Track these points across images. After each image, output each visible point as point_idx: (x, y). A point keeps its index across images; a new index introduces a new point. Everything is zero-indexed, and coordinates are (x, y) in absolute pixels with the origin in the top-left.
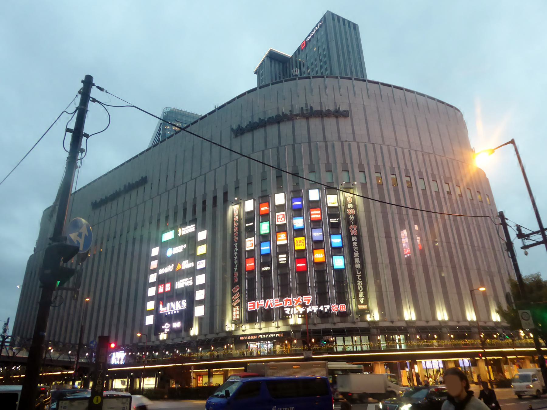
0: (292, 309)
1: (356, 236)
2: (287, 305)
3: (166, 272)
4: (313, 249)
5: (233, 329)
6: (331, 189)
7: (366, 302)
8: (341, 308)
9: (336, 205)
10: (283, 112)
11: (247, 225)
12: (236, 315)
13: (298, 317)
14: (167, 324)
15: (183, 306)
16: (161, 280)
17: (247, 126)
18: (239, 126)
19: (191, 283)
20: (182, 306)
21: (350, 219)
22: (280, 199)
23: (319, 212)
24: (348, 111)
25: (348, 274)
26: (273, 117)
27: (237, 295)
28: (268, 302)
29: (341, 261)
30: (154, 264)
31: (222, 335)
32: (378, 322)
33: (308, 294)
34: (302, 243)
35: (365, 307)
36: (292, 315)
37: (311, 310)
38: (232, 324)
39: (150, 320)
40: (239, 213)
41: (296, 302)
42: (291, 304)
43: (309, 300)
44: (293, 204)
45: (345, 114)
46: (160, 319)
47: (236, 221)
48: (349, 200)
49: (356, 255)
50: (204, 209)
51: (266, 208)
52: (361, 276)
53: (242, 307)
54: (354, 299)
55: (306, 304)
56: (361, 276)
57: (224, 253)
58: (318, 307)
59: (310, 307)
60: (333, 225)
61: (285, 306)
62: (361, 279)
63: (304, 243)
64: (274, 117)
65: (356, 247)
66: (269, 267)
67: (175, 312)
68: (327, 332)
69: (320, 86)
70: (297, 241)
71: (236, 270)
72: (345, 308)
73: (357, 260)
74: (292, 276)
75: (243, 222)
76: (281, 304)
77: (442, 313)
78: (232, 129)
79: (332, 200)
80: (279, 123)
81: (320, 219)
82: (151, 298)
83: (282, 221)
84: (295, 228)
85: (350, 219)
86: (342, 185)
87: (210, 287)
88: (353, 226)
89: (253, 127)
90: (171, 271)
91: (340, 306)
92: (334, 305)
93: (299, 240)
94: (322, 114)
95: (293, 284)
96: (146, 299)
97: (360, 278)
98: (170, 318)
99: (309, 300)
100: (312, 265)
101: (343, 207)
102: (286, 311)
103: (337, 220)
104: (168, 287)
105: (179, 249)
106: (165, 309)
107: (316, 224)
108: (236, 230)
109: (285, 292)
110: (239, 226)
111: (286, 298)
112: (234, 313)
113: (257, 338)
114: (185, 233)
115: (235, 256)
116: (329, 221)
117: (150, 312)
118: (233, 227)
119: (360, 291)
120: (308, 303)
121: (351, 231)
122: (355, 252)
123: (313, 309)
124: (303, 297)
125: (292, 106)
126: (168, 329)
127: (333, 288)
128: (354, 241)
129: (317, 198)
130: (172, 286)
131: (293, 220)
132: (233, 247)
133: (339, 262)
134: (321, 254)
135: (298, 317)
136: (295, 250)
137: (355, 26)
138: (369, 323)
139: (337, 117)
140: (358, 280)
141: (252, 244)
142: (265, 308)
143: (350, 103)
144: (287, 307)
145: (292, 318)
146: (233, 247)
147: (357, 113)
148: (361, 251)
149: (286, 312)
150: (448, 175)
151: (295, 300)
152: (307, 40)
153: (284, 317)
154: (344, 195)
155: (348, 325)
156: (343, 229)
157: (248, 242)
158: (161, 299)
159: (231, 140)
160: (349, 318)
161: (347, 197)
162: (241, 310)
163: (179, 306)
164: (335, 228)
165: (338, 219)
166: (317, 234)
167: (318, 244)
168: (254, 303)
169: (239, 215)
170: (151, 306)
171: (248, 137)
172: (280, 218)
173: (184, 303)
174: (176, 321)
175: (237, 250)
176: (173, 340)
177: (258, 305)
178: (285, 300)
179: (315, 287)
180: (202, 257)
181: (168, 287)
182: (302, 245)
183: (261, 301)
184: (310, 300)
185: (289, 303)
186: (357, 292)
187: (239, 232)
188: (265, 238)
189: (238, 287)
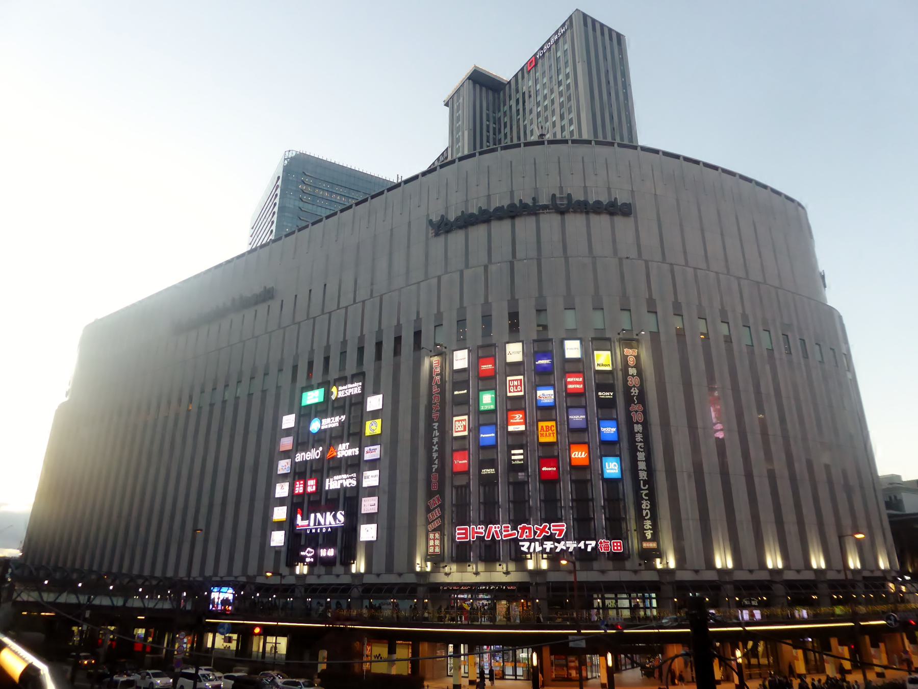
0: (533, 544)
1: (640, 423)
3: (308, 459)
5: (428, 569)
6: (601, 341)
7: (655, 538)
8: (614, 546)
9: (609, 368)
10: (521, 201)
11: (456, 393)
14: (309, 549)
15: (340, 521)
16: (299, 473)
17: (457, 219)
18: (442, 216)
19: (354, 483)
20: (337, 522)
21: (632, 394)
22: (514, 352)
23: (581, 379)
24: (630, 204)
26: (503, 206)
29: (615, 465)
30: (287, 443)
31: (410, 579)
33: (559, 520)
34: (550, 432)
35: (653, 545)
36: (531, 554)
37: (564, 548)
38: (426, 560)
39: (278, 538)
40: (442, 370)
43: (561, 531)
45: (626, 210)
46: (296, 540)
47: (436, 384)
48: (631, 361)
49: (641, 456)
50: (379, 356)
51: (490, 366)
52: (647, 492)
53: (446, 533)
54: (635, 530)
56: (647, 492)
59: (563, 543)
60: (603, 404)
63: (555, 432)
64: (505, 207)
65: (641, 442)
67: (324, 530)
69: (585, 159)
70: (542, 427)
71: (436, 469)
72: (620, 546)
73: (642, 465)
76: (514, 534)
77: (774, 557)
78: (430, 222)
79: (603, 359)
80: (513, 217)
81: (583, 391)
82: (281, 502)
83: (518, 391)
84: (539, 404)
85: (632, 394)
86: (619, 334)
87: (384, 491)
88: (636, 407)
89: (467, 222)
90: (317, 457)
91: (613, 543)
93: (546, 426)
94: (586, 208)
96: (272, 501)
97: (646, 495)
98: (316, 539)
100: (567, 470)
101: (620, 374)
102: (523, 546)
103: (610, 395)
105: (331, 422)
106: (306, 522)
108: (436, 400)
110: (442, 393)
112: (431, 543)
113: (473, 589)
114: (343, 396)
115: (435, 446)
117: (279, 526)
120: (560, 535)
121: (634, 414)
122: (639, 451)
124: (552, 524)
125: (536, 189)
126: (311, 557)
128: (638, 432)
130: (320, 485)
133: (612, 468)
134: (583, 453)
135: (543, 558)
137: (619, 37)
138: (659, 571)
139: (612, 214)
141: (465, 427)
143: (632, 191)
144: (524, 540)
147: (645, 209)
149: (522, 549)
152: (538, 56)
153: (519, 558)
154: (623, 351)
158: (297, 504)
159: (427, 239)
160: (628, 564)
161: (628, 356)
163: (330, 520)
166: (577, 418)
167: (578, 435)
168: (466, 529)
170: (280, 514)
171: (457, 238)
172: (513, 386)
173: (340, 516)
174: (327, 546)
175: (437, 434)
176: (319, 576)
178: (520, 528)
179: (572, 508)
180: (374, 440)
182: (552, 435)
184: (563, 530)
185: (528, 534)
186: (640, 518)
189: (438, 499)
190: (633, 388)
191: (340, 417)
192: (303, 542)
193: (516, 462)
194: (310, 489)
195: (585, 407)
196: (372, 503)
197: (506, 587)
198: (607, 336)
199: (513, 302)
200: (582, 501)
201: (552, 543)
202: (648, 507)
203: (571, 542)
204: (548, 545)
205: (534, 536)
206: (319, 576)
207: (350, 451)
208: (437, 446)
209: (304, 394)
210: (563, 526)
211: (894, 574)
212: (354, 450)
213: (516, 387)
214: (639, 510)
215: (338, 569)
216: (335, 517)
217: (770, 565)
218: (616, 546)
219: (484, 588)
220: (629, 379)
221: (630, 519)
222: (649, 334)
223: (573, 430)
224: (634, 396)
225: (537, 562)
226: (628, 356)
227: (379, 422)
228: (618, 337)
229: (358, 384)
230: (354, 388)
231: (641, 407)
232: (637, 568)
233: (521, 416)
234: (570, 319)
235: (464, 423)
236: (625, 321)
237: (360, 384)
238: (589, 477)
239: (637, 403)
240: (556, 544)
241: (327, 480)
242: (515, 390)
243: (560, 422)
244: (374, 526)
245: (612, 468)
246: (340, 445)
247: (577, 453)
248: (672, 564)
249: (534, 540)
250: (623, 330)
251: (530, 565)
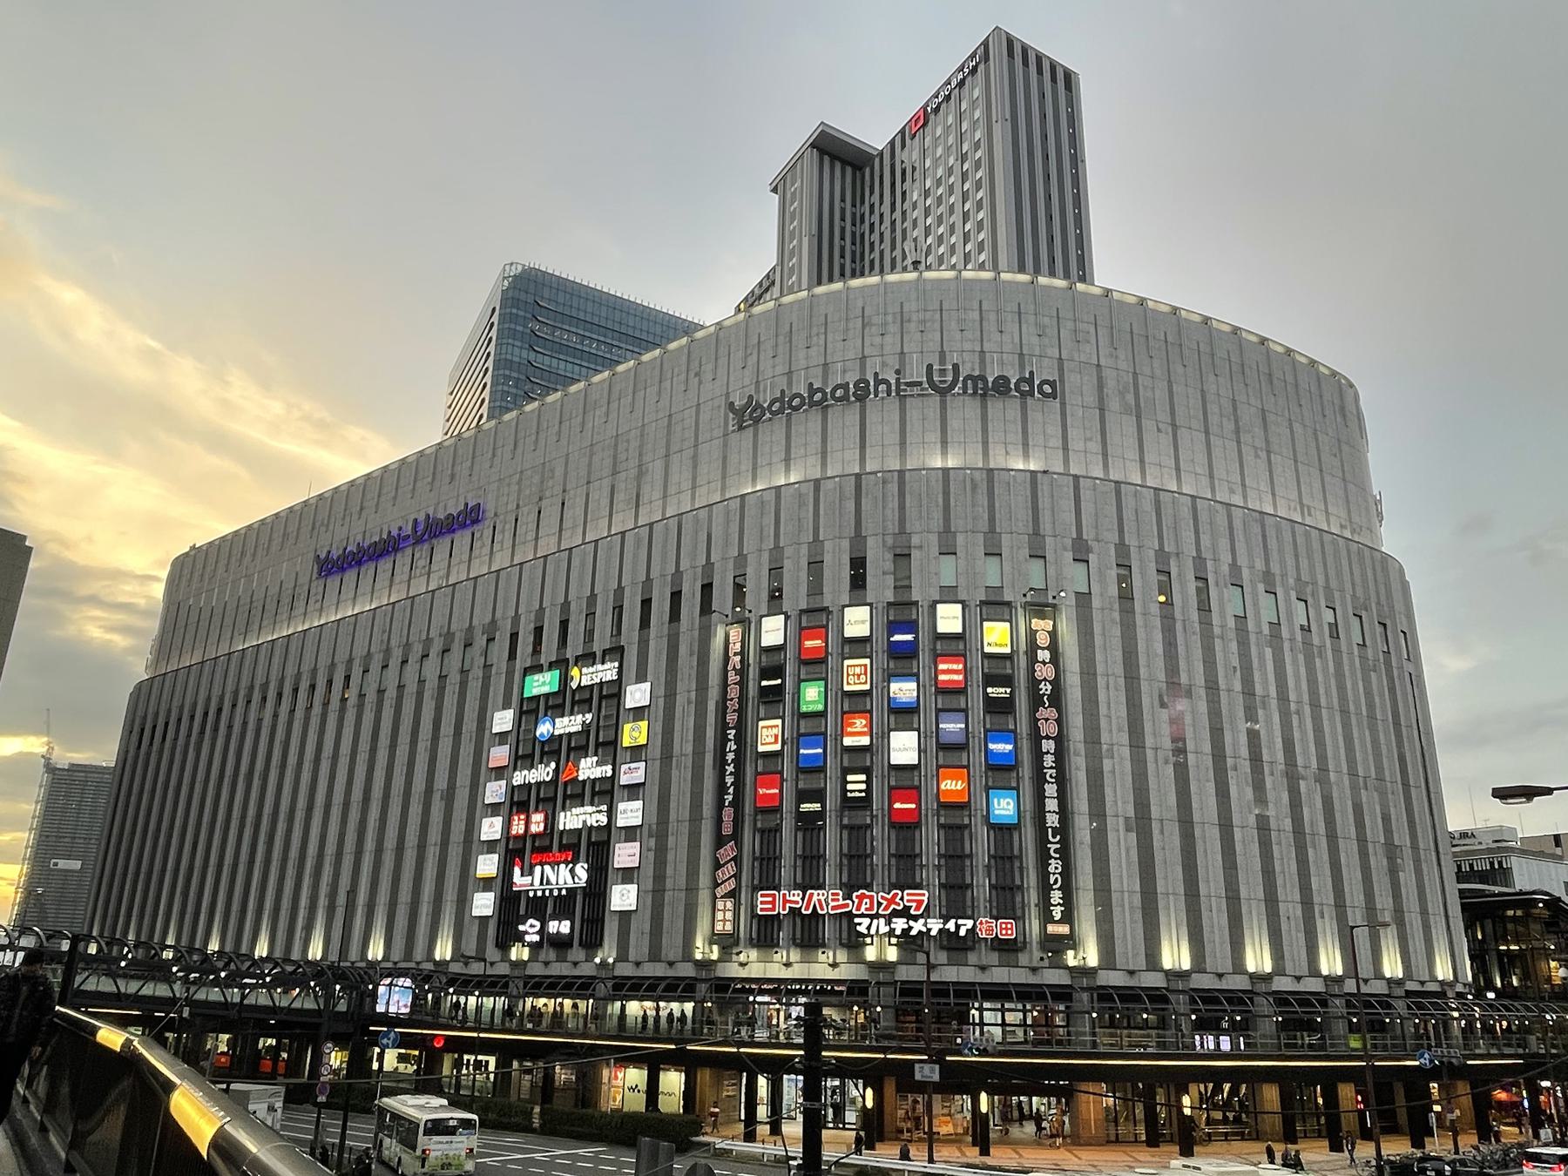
0: (875, 921)
2: (863, 910)
5: (715, 956)
6: (995, 606)
7: (1068, 918)
9: (1007, 650)
11: (764, 683)
12: (724, 920)
14: (531, 921)
15: (580, 879)
16: (519, 802)
19: (604, 820)
20: (576, 880)
22: (857, 622)
23: (961, 667)
28: (812, 895)
29: (1008, 803)
35: (1064, 929)
36: (872, 936)
37: (924, 930)
38: (711, 944)
39: (484, 904)
40: (743, 647)
41: (885, 903)
42: (871, 908)
43: (920, 903)
44: (892, 639)
46: (512, 907)
47: (734, 668)
48: (1043, 639)
49: (1051, 789)
50: (645, 622)
52: (1058, 846)
53: (743, 901)
55: (912, 912)
56: (1058, 846)
57: (698, 753)
59: (922, 921)
60: (993, 705)
61: (854, 912)
62: (1058, 856)
65: (1051, 768)
66: (819, 805)
67: (556, 893)
68: (967, 992)
73: (1052, 805)
75: (753, 672)
76: (847, 905)
79: (997, 637)
82: (491, 846)
83: (861, 683)
88: (1045, 712)
90: (548, 779)
92: (984, 920)
96: (472, 845)
97: (1055, 851)
98: (539, 907)
99: (920, 903)
102: (860, 924)
104: (538, 823)
105: (569, 724)
108: (733, 692)
111: (861, 891)
112: (720, 916)
113: (782, 990)
114: (590, 683)
115: (729, 765)
117: (486, 884)
120: (917, 909)
121: (1042, 724)
122: (1049, 782)
123: (929, 926)
124: (906, 892)
128: (1048, 753)
129: (956, 627)
130: (550, 822)
132: (722, 740)
133: (1004, 807)
134: (960, 782)
135: (890, 944)
137: (1069, 77)
140: (1051, 857)
141: (776, 736)
142: (804, 912)
144: (863, 916)
145: (872, 944)
148: (1062, 781)
149: (858, 928)
150: (1305, 577)
151: (882, 897)
152: (929, 109)
153: (854, 943)
155: (1019, 976)
157: (765, 730)
158: (514, 851)
160: (1023, 959)
161: (1037, 631)
163: (567, 876)
165: (1008, 690)
169: (742, 653)
172: (854, 675)
173: (582, 872)
174: (558, 917)
175: (734, 747)
176: (546, 964)
177: (785, 901)
178: (857, 897)
179: (939, 867)
180: (636, 752)
181: (538, 823)
183: (792, 892)
185: (868, 906)
189: (732, 849)
191: (584, 716)
192: (522, 912)
193: (853, 795)
194: (534, 829)
195: (965, 711)
196: (631, 851)
197: (832, 987)
198: (1007, 598)
199: (858, 539)
200: (955, 858)
201: (905, 920)
203: (935, 921)
204: (900, 924)
205: (878, 909)
206: (546, 964)
207: (599, 769)
209: (528, 679)
210: (924, 895)
211: (1459, 988)
212: (604, 768)
213: (859, 676)
214: (1044, 875)
215: (577, 953)
216: (572, 871)
217: (1251, 967)
219: (798, 987)
220: (1038, 667)
221: (1029, 887)
222: (1073, 596)
223: (944, 747)
224: (1044, 694)
225: (881, 950)
226: (1037, 631)
227: (644, 725)
228: (1024, 600)
229: (613, 665)
230: (606, 672)
231: (1052, 713)
232: (1035, 964)
233: (864, 722)
234: (948, 570)
235: (775, 731)
236: (1035, 575)
237: (616, 664)
238: (966, 821)
240: (912, 923)
241: (562, 814)
242: (857, 681)
243: (925, 732)
244: (633, 888)
246: (583, 760)
247: (949, 782)
248: (1093, 960)
249: (877, 916)
250: (1031, 589)
251: (871, 954)
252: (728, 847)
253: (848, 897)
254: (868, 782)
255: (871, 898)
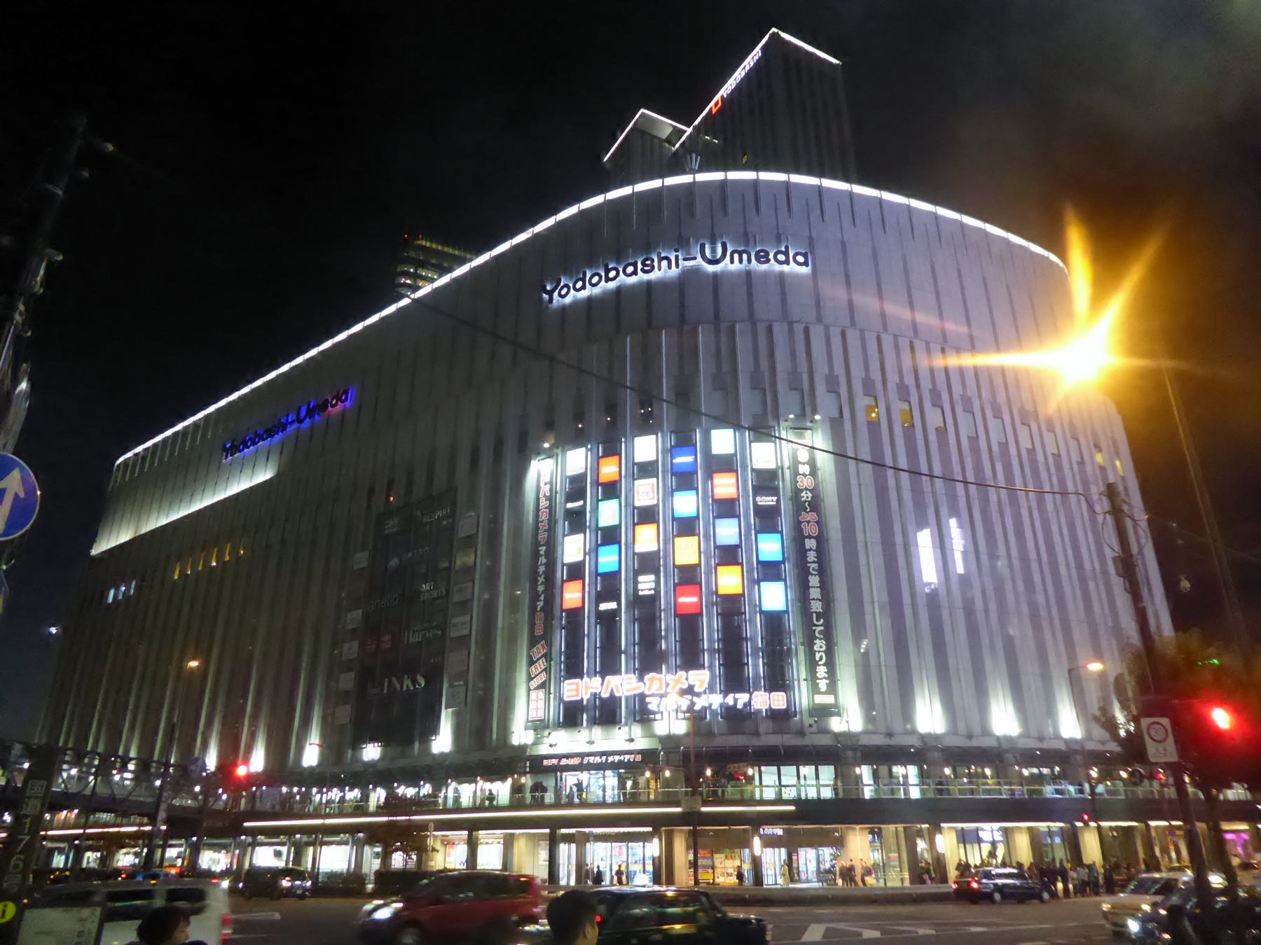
2: (653, 691)
4: (717, 565)
6: (762, 430)
7: (832, 689)
8: (774, 700)
11: (570, 505)
13: (677, 719)
25: (793, 623)
27: (541, 664)
28: (609, 681)
32: (856, 735)
33: (702, 667)
35: (829, 699)
36: (662, 713)
43: (702, 682)
47: (545, 496)
48: (803, 455)
49: (814, 581)
52: (822, 628)
53: (552, 691)
54: (804, 680)
56: (822, 628)
58: (722, 696)
59: (704, 696)
65: (814, 562)
73: (815, 593)
74: (667, 623)
75: (560, 498)
79: (763, 455)
95: (669, 642)
97: (820, 632)
101: (787, 473)
107: (727, 508)
108: (544, 516)
109: (650, 660)
110: (551, 509)
112: (532, 705)
115: (540, 576)
116: (755, 503)
118: (537, 509)
119: (820, 663)
120: (701, 686)
121: (805, 525)
122: (812, 575)
127: (758, 655)
128: (810, 549)
131: (672, 496)
133: (774, 596)
136: (675, 566)
138: (837, 736)
140: (817, 638)
146: (536, 555)
148: (823, 572)
155: (789, 740)
156: (785, 522)
162: (549, 698)
164: (767, 520)
165: (775, 499)
166: (727, 531)
167: (729, 555)
169: (551, 483)
177: (587, 688)
178: (649, 679)
186: (812, 665)
187: (552, 521)
188: (610, 536)
189: (543, 648)
190: (804, 492)
202: (824, 648)
208: (543, 576)
213: (647, 493)
218: (778, 701)
224: (805, 501)
231: (812, 516)
239: (810, 511)
240: (695, 699)
245: (774, 596)
252: (539, 646)
253: (641, 679)
254: (657, 582)
255: (660, 680)
